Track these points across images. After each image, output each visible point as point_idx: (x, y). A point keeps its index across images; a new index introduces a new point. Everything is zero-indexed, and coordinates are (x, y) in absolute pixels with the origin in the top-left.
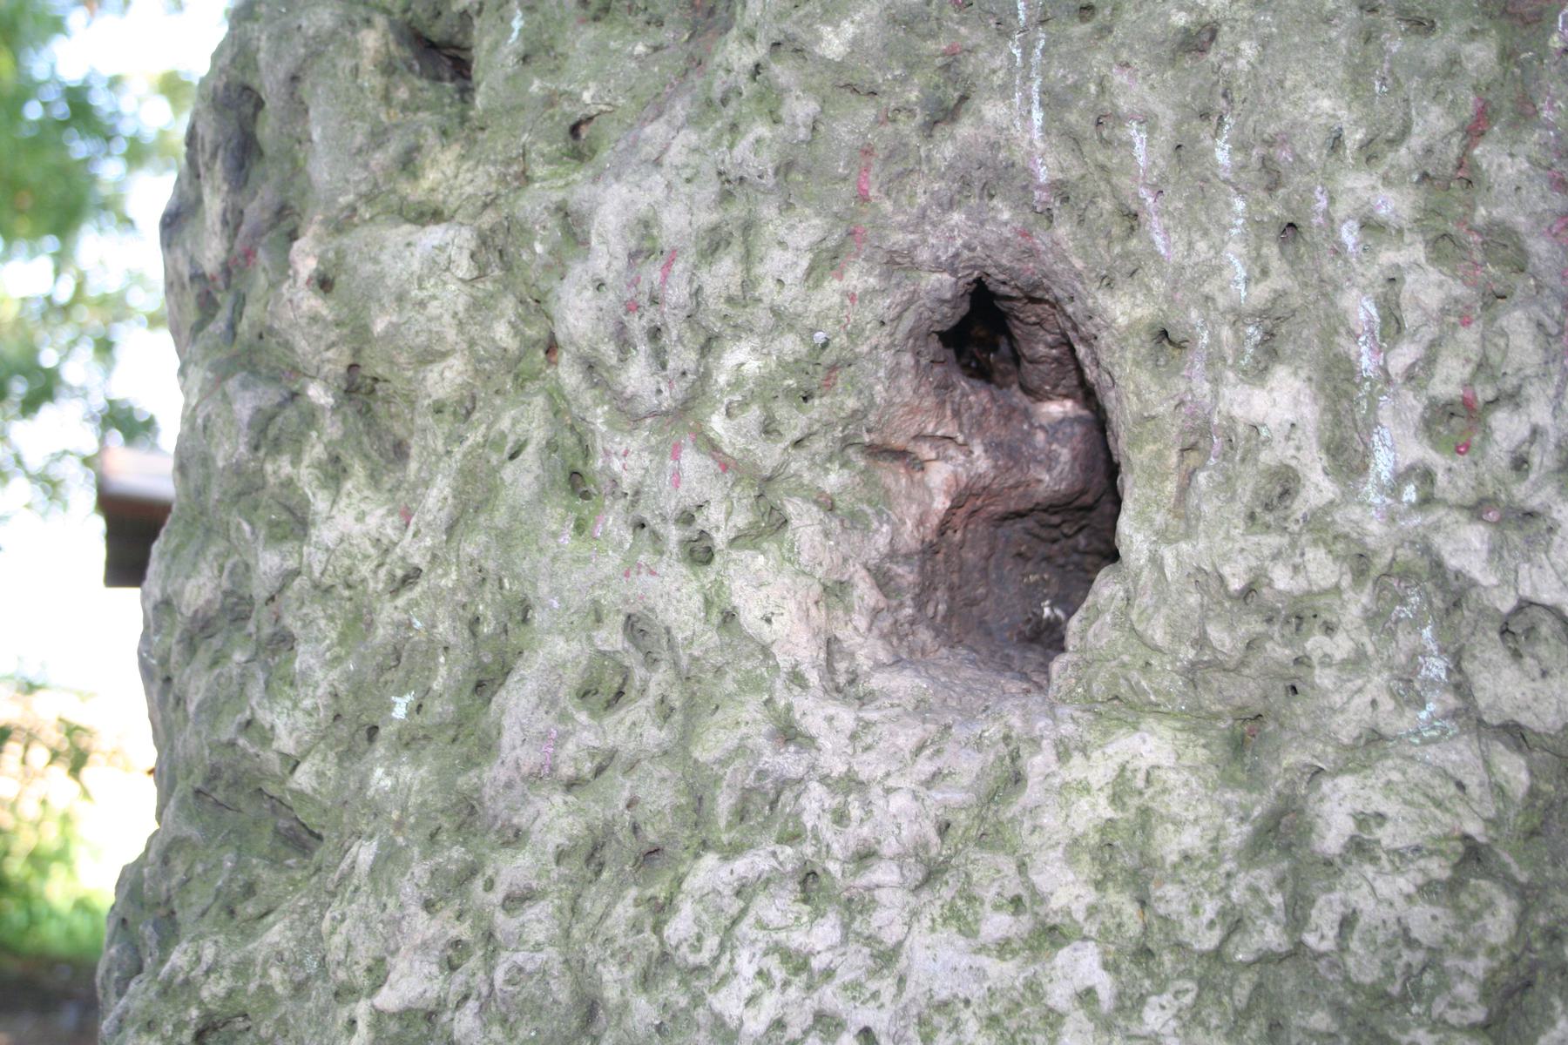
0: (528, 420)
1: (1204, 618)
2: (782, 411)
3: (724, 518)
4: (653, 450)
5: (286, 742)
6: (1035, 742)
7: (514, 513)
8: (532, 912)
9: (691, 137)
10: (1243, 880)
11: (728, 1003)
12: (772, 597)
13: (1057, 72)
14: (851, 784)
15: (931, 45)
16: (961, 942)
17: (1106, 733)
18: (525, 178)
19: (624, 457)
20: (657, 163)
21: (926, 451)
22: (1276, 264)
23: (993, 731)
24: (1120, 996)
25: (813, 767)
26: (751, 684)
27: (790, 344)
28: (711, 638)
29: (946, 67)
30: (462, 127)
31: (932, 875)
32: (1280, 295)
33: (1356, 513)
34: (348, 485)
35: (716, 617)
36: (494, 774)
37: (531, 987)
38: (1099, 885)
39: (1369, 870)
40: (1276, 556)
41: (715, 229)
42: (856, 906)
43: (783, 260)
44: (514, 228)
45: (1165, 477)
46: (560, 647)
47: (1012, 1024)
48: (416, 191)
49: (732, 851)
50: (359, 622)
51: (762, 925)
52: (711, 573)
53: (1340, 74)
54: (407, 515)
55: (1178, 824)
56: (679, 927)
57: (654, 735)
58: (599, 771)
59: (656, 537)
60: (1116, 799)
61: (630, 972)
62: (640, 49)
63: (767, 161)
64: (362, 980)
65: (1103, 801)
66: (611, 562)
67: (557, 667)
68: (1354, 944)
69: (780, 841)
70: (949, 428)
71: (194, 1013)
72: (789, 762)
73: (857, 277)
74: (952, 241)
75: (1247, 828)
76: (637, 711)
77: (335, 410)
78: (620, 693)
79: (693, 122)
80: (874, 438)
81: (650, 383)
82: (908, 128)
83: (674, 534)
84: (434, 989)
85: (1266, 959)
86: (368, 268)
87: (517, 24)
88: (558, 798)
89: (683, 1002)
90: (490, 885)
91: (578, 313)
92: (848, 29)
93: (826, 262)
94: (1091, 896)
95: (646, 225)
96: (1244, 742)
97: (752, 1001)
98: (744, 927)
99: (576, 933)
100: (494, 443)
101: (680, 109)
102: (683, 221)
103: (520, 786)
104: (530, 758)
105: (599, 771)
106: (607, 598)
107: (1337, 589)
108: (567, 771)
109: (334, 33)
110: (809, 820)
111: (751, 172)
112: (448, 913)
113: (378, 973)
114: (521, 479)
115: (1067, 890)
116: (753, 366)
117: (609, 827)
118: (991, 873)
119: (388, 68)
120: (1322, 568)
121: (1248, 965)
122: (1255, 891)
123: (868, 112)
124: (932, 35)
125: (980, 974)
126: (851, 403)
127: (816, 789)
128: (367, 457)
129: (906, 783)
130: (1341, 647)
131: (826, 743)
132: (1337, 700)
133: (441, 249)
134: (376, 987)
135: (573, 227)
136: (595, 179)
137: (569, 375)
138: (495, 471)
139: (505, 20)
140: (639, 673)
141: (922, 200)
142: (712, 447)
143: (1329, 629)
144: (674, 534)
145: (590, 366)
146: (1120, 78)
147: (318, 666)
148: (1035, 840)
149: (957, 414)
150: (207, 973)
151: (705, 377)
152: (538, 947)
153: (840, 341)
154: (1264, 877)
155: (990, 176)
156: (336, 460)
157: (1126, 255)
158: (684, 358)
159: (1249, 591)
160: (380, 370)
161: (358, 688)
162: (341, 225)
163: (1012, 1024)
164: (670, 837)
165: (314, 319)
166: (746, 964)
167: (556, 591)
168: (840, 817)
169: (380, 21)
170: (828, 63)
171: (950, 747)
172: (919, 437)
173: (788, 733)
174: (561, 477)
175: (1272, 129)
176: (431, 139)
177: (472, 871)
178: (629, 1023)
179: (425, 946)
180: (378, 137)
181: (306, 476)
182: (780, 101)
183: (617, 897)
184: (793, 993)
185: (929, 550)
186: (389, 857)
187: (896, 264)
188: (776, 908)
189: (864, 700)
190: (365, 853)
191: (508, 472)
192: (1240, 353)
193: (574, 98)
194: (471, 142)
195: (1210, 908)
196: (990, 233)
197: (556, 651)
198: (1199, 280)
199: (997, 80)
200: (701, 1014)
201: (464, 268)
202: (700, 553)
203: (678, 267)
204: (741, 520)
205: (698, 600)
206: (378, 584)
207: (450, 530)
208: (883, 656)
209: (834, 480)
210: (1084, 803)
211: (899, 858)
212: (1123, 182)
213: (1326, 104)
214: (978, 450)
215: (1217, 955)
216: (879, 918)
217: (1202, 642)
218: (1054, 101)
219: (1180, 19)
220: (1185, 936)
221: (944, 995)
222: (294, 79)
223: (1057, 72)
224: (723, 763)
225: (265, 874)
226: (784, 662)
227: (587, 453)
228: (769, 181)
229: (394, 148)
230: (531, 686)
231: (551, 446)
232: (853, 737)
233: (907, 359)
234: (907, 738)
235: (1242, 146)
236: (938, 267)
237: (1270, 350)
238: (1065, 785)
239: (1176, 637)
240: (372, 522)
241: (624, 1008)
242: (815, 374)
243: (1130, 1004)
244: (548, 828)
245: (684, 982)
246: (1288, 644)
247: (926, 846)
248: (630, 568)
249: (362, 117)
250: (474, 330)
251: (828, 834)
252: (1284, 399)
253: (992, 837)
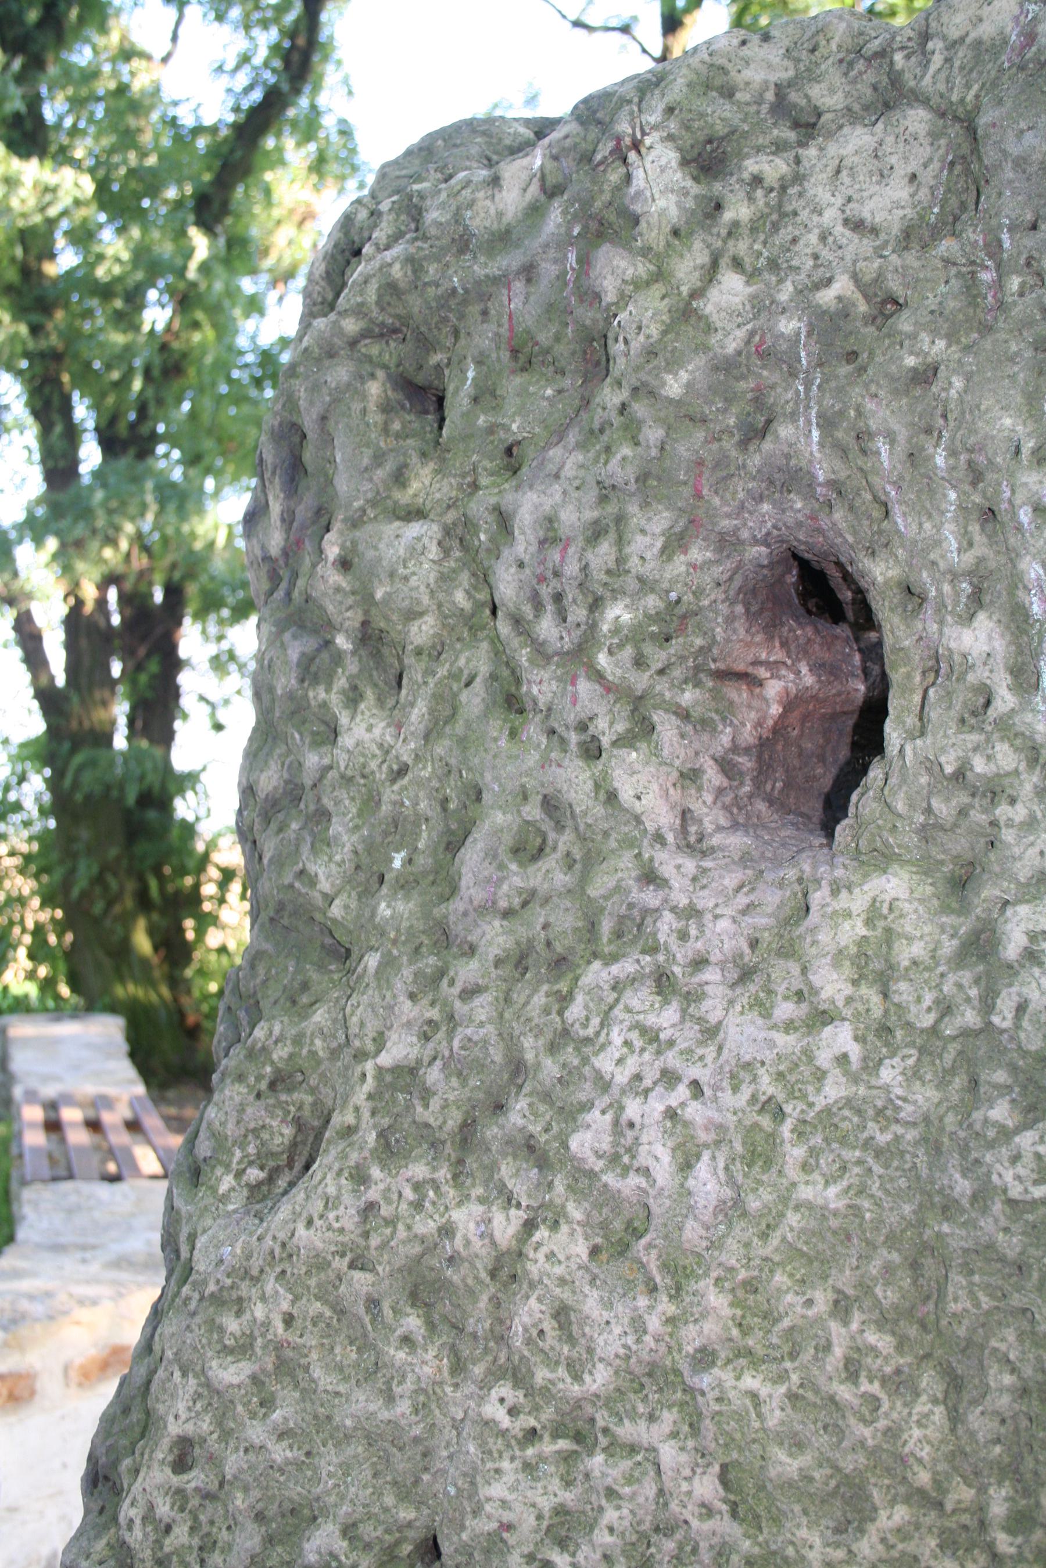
0: (478, 660)
1: (930, 794)
2: (648, 649)
4: (559, 680)
5: (325, 885)
6: (818, 882)
7: (468, 726)
8: (478, 1001)
9: (579, 457)
10: (951, 978)
11: (604, 1063)
12: (643, 784)
13: (828, 401)
14: (692, 912)
15: (743, 385)
16: (760, 1021)
17: (866, 876)
18: (475, 486)
19: (541, 686)
20: (557, 476)
21: (763, 673)
22: (978, 538)
23: (791, 874)
24: (865, 1059)
25: (666, 901)
26: (628, 842)
27: (652, 602)
28: (599, 810)
29: (756, 400)
30: (434, 448)
31: (746, 975)
32: (981, 560)
33: (1029, 717)
34: (362, 706)
35: (602, 796)
36: (458, 905)
37: (477, 1052)
38: (855, 983)
39: (1036, 971)
40: (975, 749)
41: (596, 522)
42: (693, 997)
43: (645, 543)
44: (468, 523)
45: (912, 691)
46: (499, 818)
47: (792, 1078)
48: (403, 497)
49: (613, 958)
50: (371, 802)
51: (628, 1010)
52: (599, 765)
53: (1019, 399)
54: (399, 726)
55: (910, 939)
56: (575, 1011)
57: (561, 879)
58: (525, 904)
59: (563, 741)
60: (869, 922)
61: (541, 1042)
62: (549, 392)
63: (631, 473)
64: (370, 1046)
65: (859, 923)
66: (533, 758)
67: (497, 832)
68: (1025, 1024)
69: (643, 952)
70: (778, 655)
71: (268, 1069)
72: (650, 898)
73: (698, 553)
74: (763, 523)
75: (955, 942)
76: (551, 862)
77: (354, 653)
78: (541, 850)
79: (581, 446)
80: (721, 665)
81: (555, 632)
82: (729, 444)
83: (574, 738)
84: (414, 1053)
85: (966, 1033)
86: (370, 554)
87: (471, 374)
88: (497, 923)
89: (576, 1062)
90: (452, 983)
91: (508, 585)
92: (684, 376)
93: (675, 543)
94: (848, 990)
95: (550, 521)
96: (961, 883)
97: (620, 1061)
98: (618, 1012)
99: (507, 1015)
100: (454, 676)
101: (573, 437)
102: (574, 518)
103: (473, 915)
104: (478, 895)
105: (525, 904)
106: (530, 783)
107: (1016, 772)
108: (503, 904)
109: (349, 384)
110: (662, 938)
111: (619, 481)
112: (425, 1002)
113: (380, 1042)
114: (473, 700)
115: (832, 985)
116: (626, 617)
117: (530, 941)
118: (785, 974)
119: (386, 408)
120: (1007, 757)
121: (954, 1038)
122: (960, 986)
123: (700, 435)
124: (743, 377)
125: (771, 1044)
126: (699, 642)
127: (668, 916)
128: (376, 685)
129: (729, 911)
130: (1019, 813)
131: (675, 884)
132: (1017, 851)
133: (419, 539)
134: (379, 1051)
135: (504, 521)
136: (518, 488)
137: (504, 627)
138: (455, 695)
139: (463, 372)
140: (552, 835)
141: (741, 495)
142: (599, 676)
143: (1013, 801)
144: (574, 738)
145: (517, 621)
146: (870, 405)
147: (345, 833)
148: (813, 951)
149: (784, 644)
150: (276, 1042)
151: (593, 626)
152: (481, 1024)
153: (688, 598)
154: (966, 976)
155: (787, 478)
156: (354, 688)
157: (880, 532)
158: (578, 613)
159: (960, 775)
160: (382, 625)
161: (371, 847)
162: (355, 523)
163: (792, 1078)
164: (571, 949)
165: (338, 589)
166: (617, 1037)
167: (497, 779)
168: (683, 936)
169: (380, 374)
170: (670, 401)
171: (761, 886)
172: (757, 663)
173: (650, 877)
174: (500, 699)
175: (972, 440)
176: (414, 459)
177: (442, 973)
178: (540, 1076)
179: (409, 1024)
180: (379, 459)
181: (335, 699)
182: (639, 429)
183: (535, 991)
184: (647, 1056)
185: (763, 744)
186: (388, 963)
187: (726, 543)
188: (641, 998)
189: (704, 854)
190: (372, 961)
191: (464, 696)
192: (956, 603)
193: (507, 429)
194: (443, 460)
195: (928, 998)
196: (789, 518)
197: (497, 820)
198: (926, 551)
199: (789, 409)
200: (587, 1070)
201: (434, 552)
202: (592, 751)
203: (571, 550)
204: (620, 727)
205: (589, 785)
206: (382, 775)
207: (427, 737)
208: (723, 822)
209: (688, 697)
210: (847, 925)
211: (722, 965)
212: (875, 480)
213: (1008, 422)
214: (804, 670)
215: (934, 1030)
216: (706, 1005)
217: (929, 810)
218: (828, 423)
219: (911, 361)
220: (911, 1018)
221: (748, 1058)
222: (324, 418)
223: (828, 401)
224: (606, 898)
225: (314, 975)
226: (651, 827)
227: (518, 682)
228: (633, 487)
229: (389, 466)
230: (480, 845)
231: (493, 677)
232: (694, 879)
233: (739, 609)
234: (730, 881)
235: (953, 453)
236: (756, 541)
237: (977, 600)
238: (835, 912)
239: (912, 806)
240: (377, 732)
241: (538, 1065)
242: (672, 621)
243: (871, 1065)
244: (490, 943)
245: (577, 1049)
246: (985, 811)
247: (741, 956)
248: (545, 763)
249: (367, 445)
250: (441, 596)
251: (674, 948)
252: (983, 636)
253: (788, 950)
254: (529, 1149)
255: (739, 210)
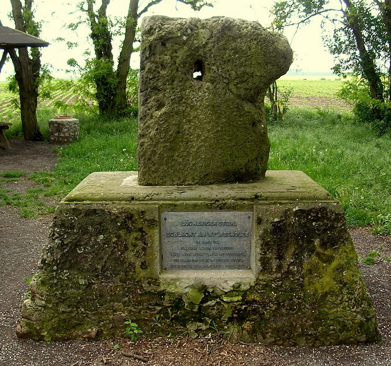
3: (186, 73)
254: (185, 103)
255: (195, 35)
